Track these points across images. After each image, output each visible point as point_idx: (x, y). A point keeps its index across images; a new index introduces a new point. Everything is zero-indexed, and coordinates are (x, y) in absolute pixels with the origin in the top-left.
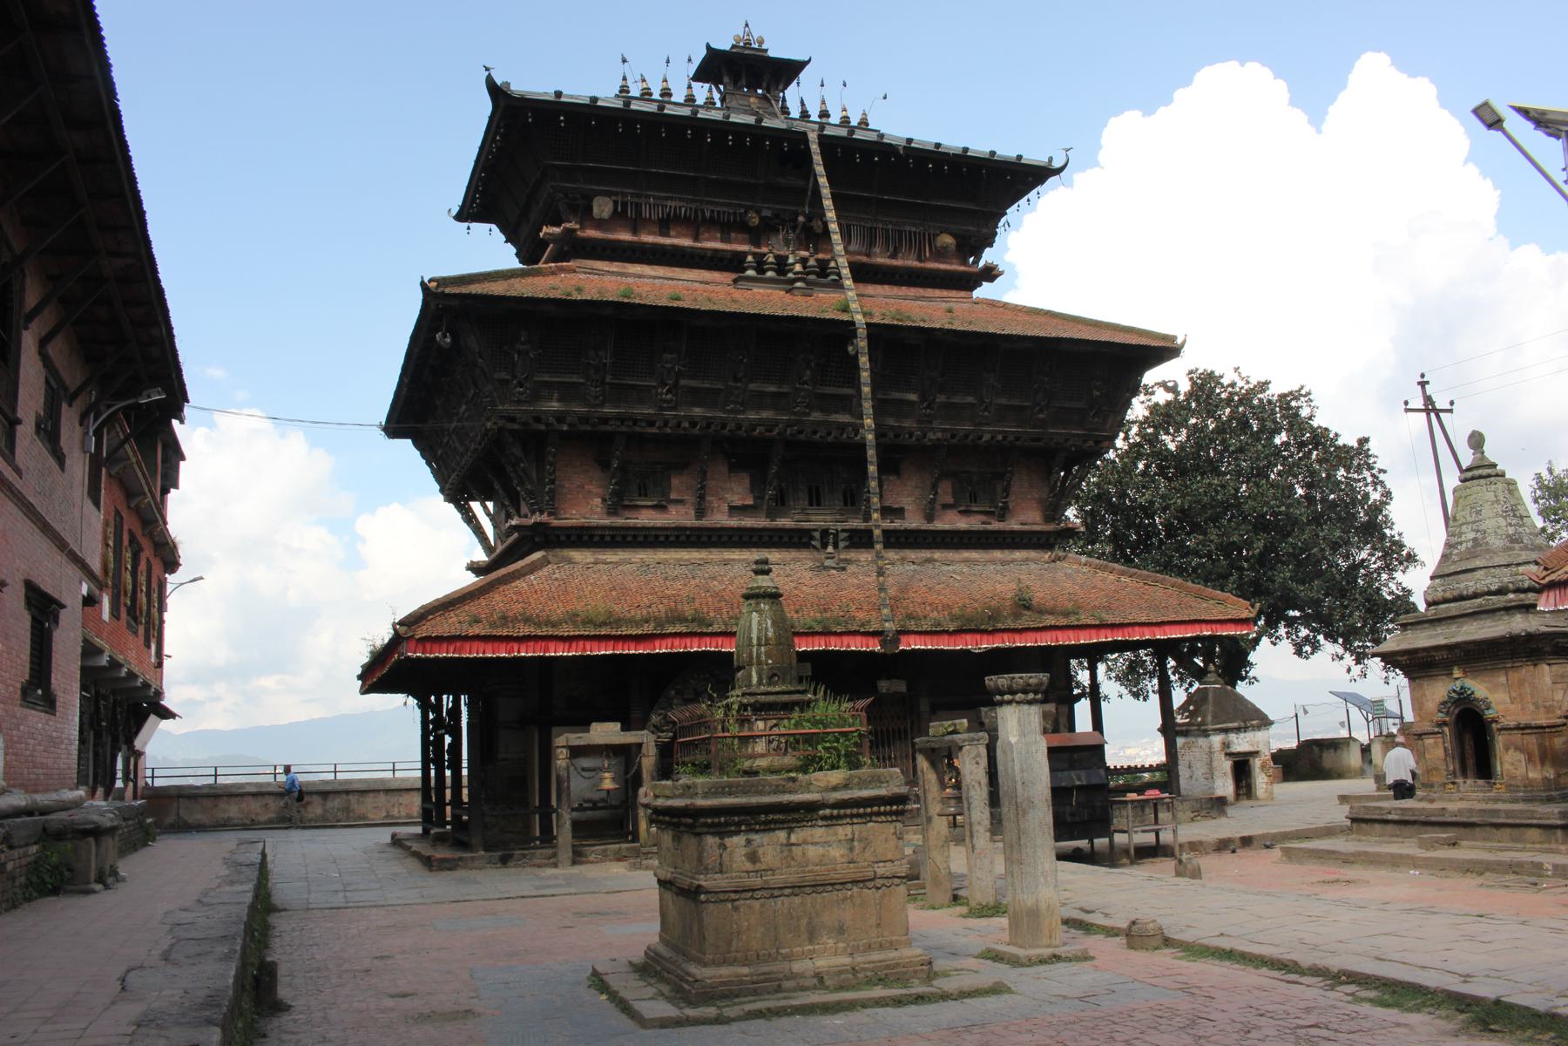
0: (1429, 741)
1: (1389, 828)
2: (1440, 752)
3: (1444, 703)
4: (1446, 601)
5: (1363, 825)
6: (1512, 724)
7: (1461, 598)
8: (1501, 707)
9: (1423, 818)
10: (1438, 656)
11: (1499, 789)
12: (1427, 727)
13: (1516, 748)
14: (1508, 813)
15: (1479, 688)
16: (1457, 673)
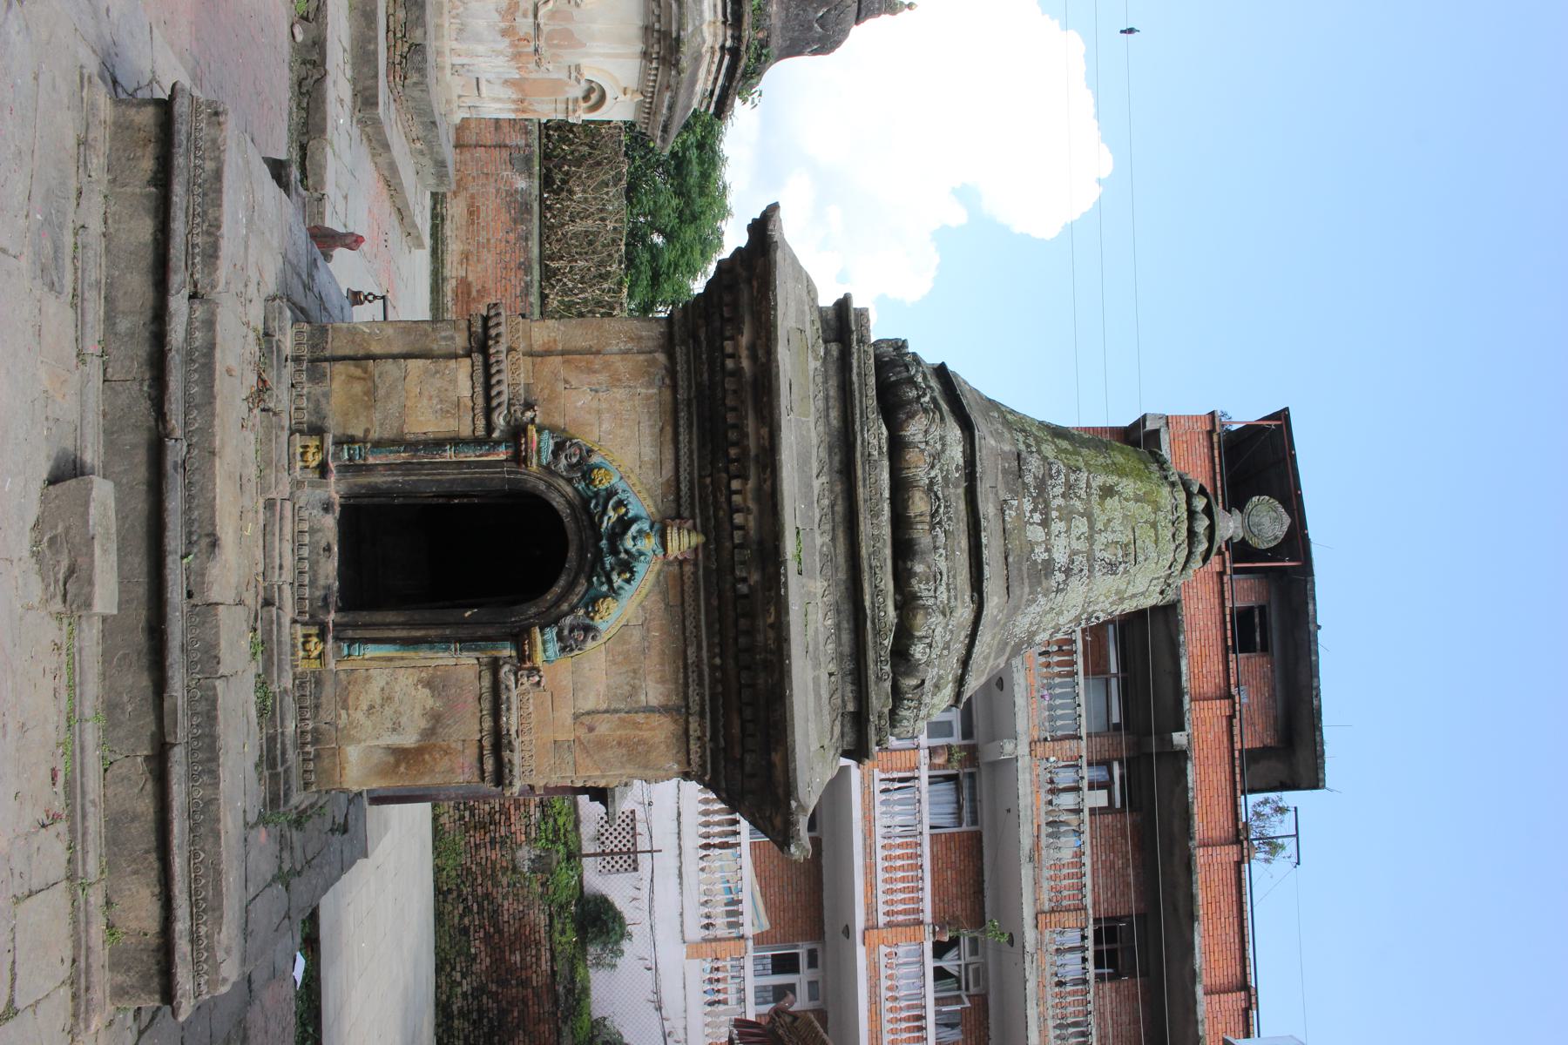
0: (462, 378)
1: (138, 285)
2: (426, 422)
3: (584, 468)
4: (900, 487)
5: (147, 164)
6: (511, 721)
7: (904, 549)
8: (566, 680)
9: (176, 451)
10: (744, 491)
11: (300, 653)
12: (513, 376)
13: (436, 718)
14: (205, 815)
15: (631, 609)
16: (682, 542)
